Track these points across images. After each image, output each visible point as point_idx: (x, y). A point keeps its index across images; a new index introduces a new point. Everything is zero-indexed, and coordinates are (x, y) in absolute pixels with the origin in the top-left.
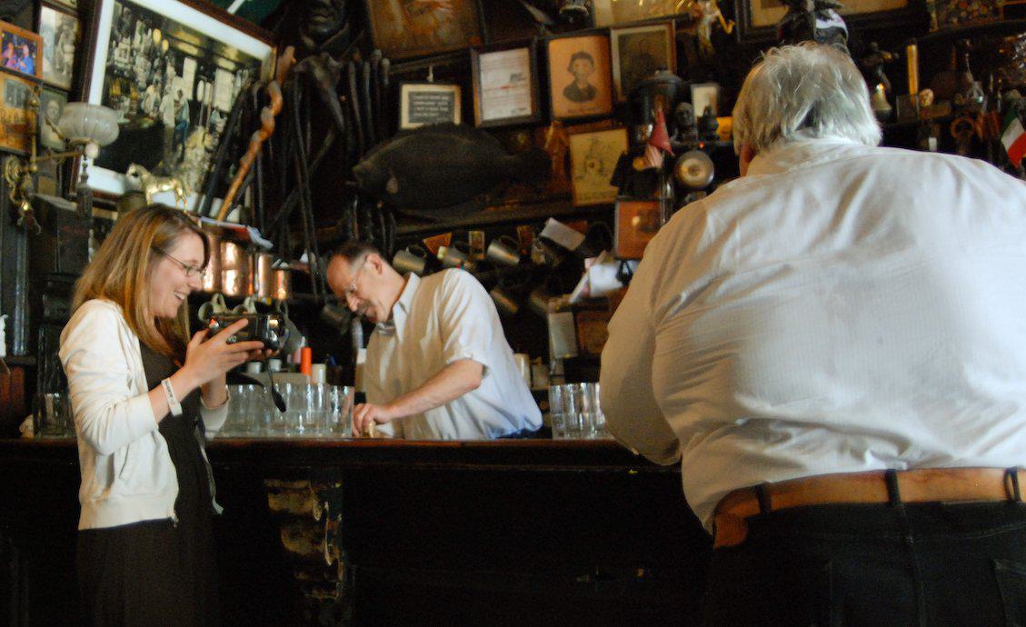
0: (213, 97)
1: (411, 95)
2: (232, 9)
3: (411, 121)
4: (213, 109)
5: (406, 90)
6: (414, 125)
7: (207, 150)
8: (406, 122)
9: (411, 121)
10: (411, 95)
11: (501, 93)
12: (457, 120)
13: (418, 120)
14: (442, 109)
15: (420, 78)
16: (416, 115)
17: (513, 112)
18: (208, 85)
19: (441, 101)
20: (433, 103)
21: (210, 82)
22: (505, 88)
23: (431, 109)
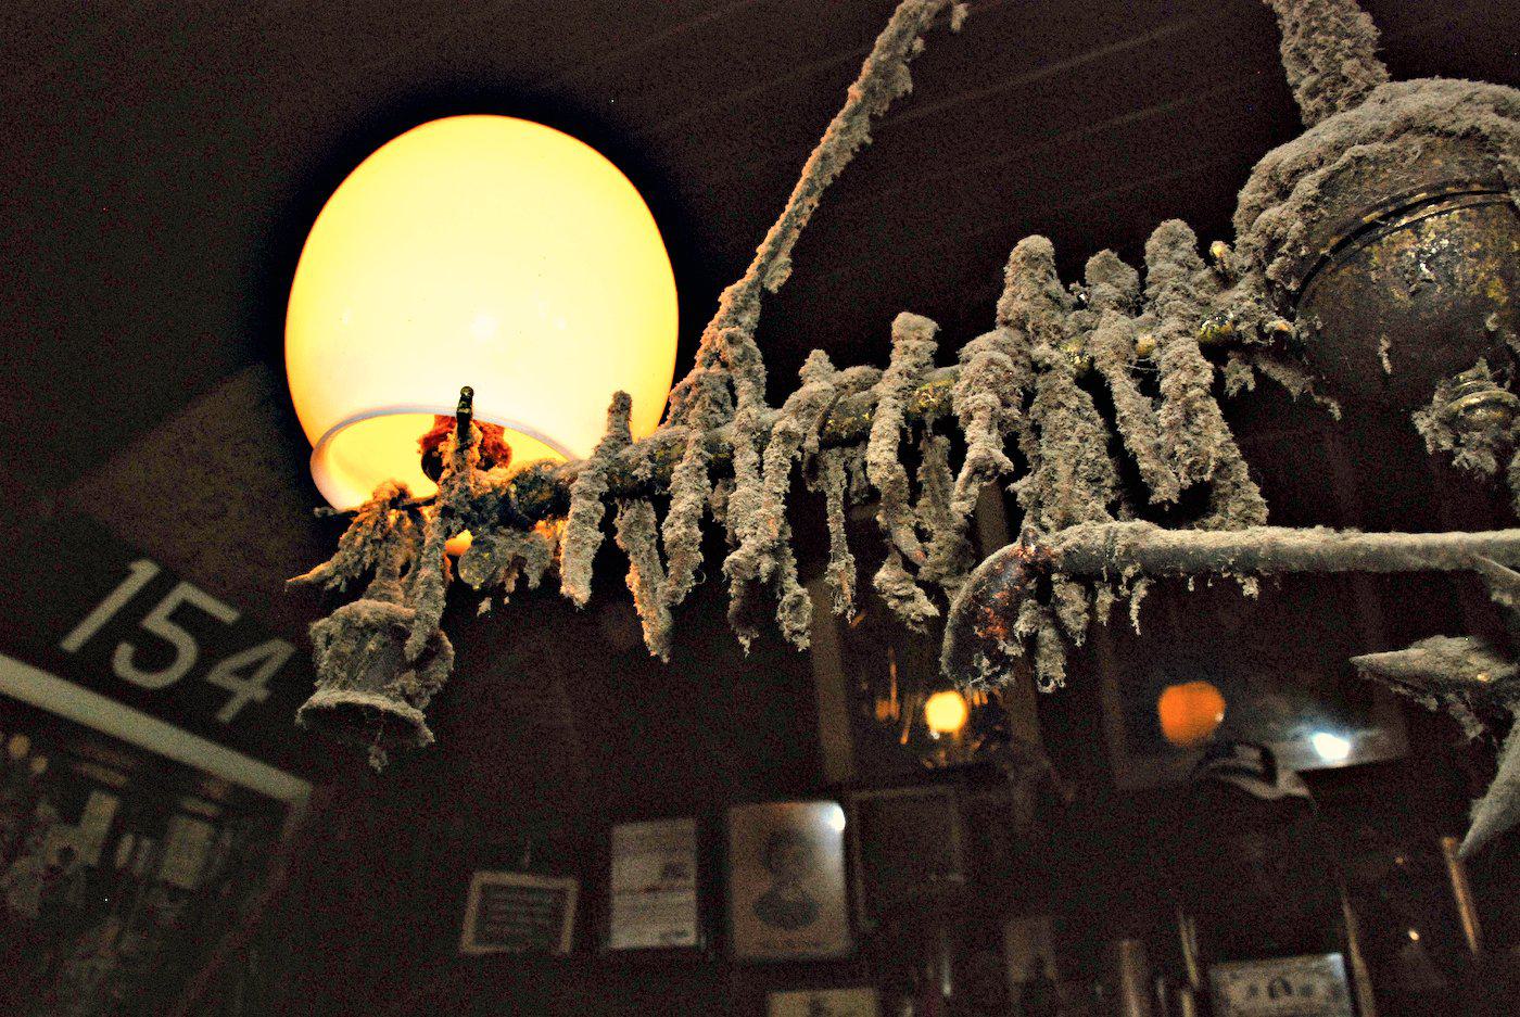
0: (157, 864)
1: (485, 889)
2: (227, 714)
3: (478, 941)
4: (151, 884)
5: (482, 878)
6: (481, 950)
7: (123, 959)
8: (469, 943)
9: (478, 941)
10: (485, 889)
11: (644, 900)
12: (566, 944)
13: (490, 939)
14: (539, 921)
15: (505, 860)
16: (488, 929)
17: (663, 936)
18: (146, 843)
19: (540, 904)
20: (523, 909)
21: (149, 835)
22: (651, 890)
23: (521, 919)
